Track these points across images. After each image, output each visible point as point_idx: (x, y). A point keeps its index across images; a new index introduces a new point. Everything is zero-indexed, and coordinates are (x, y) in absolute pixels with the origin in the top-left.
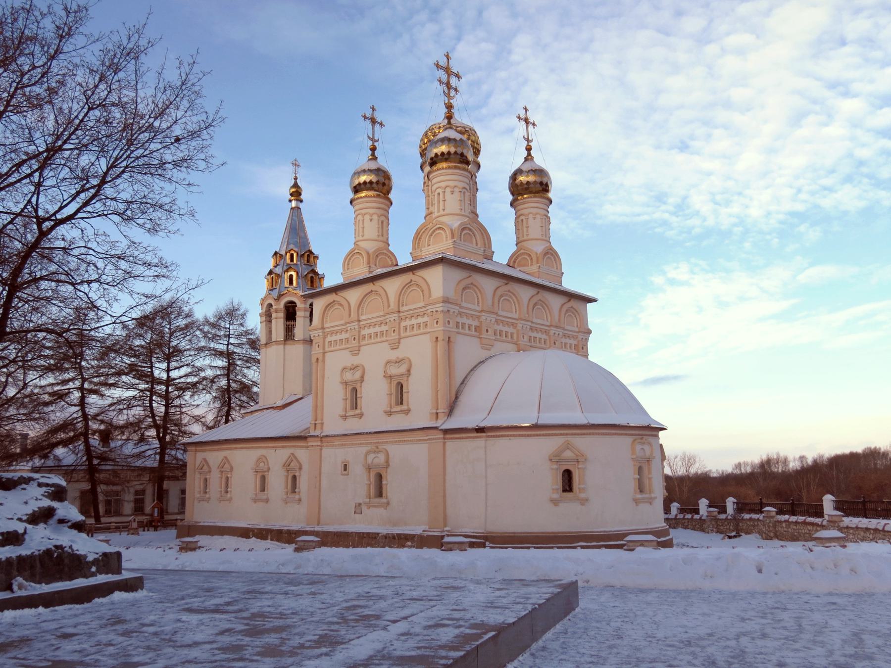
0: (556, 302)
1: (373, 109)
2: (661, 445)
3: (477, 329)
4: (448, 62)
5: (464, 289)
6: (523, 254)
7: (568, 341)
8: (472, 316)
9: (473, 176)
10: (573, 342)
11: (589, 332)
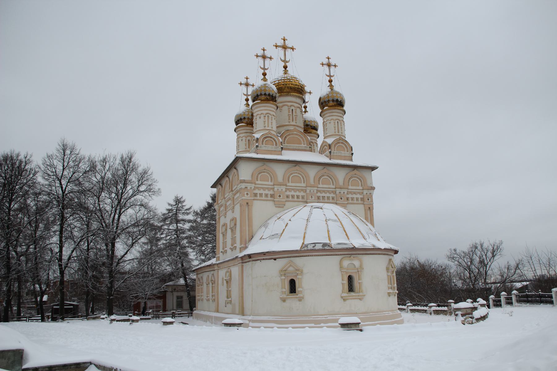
1: (247, 78)
3: (272, 196)
4: (285, 43)
7: (355, 196)
8: (268, 188)
10: (359, 196)
11: (373, 188)
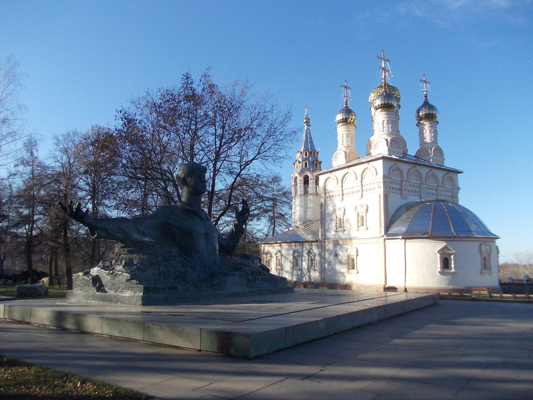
0: (440, 174)
2: (497, 247)
5: (393, 171)
6: (424, 150)
7: (447, 193)
9: (397, 113)
11: (459, 189)
